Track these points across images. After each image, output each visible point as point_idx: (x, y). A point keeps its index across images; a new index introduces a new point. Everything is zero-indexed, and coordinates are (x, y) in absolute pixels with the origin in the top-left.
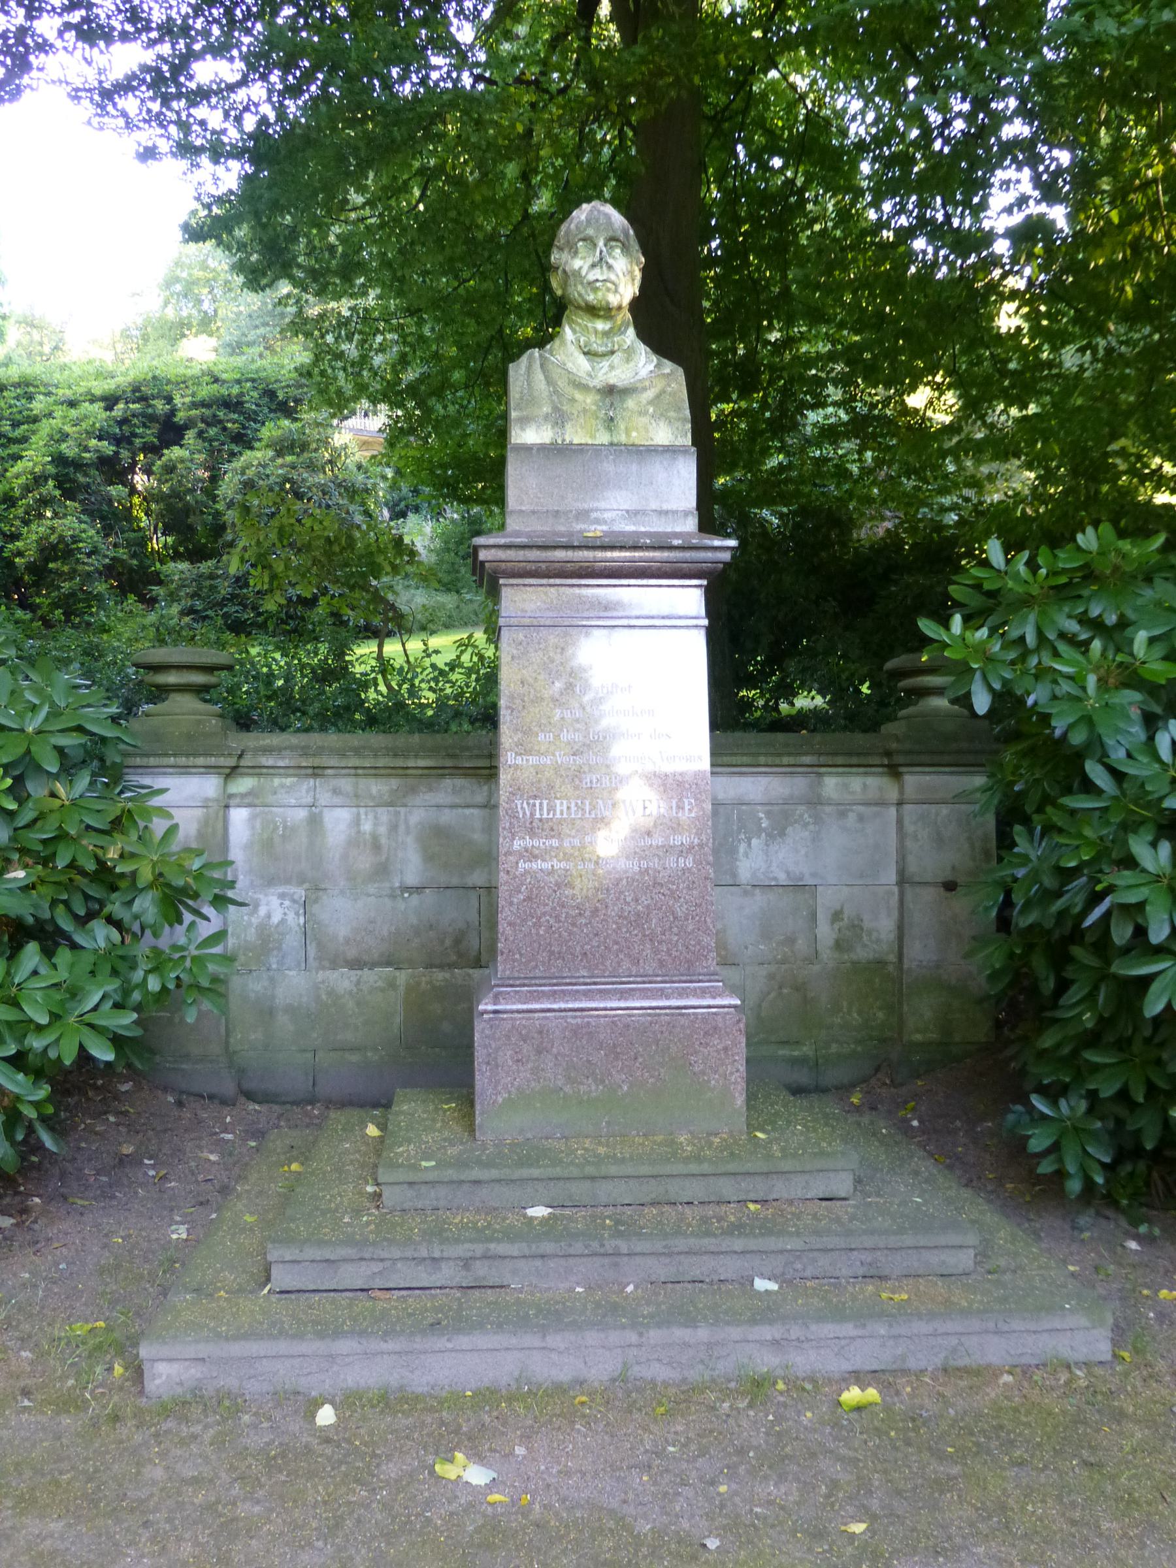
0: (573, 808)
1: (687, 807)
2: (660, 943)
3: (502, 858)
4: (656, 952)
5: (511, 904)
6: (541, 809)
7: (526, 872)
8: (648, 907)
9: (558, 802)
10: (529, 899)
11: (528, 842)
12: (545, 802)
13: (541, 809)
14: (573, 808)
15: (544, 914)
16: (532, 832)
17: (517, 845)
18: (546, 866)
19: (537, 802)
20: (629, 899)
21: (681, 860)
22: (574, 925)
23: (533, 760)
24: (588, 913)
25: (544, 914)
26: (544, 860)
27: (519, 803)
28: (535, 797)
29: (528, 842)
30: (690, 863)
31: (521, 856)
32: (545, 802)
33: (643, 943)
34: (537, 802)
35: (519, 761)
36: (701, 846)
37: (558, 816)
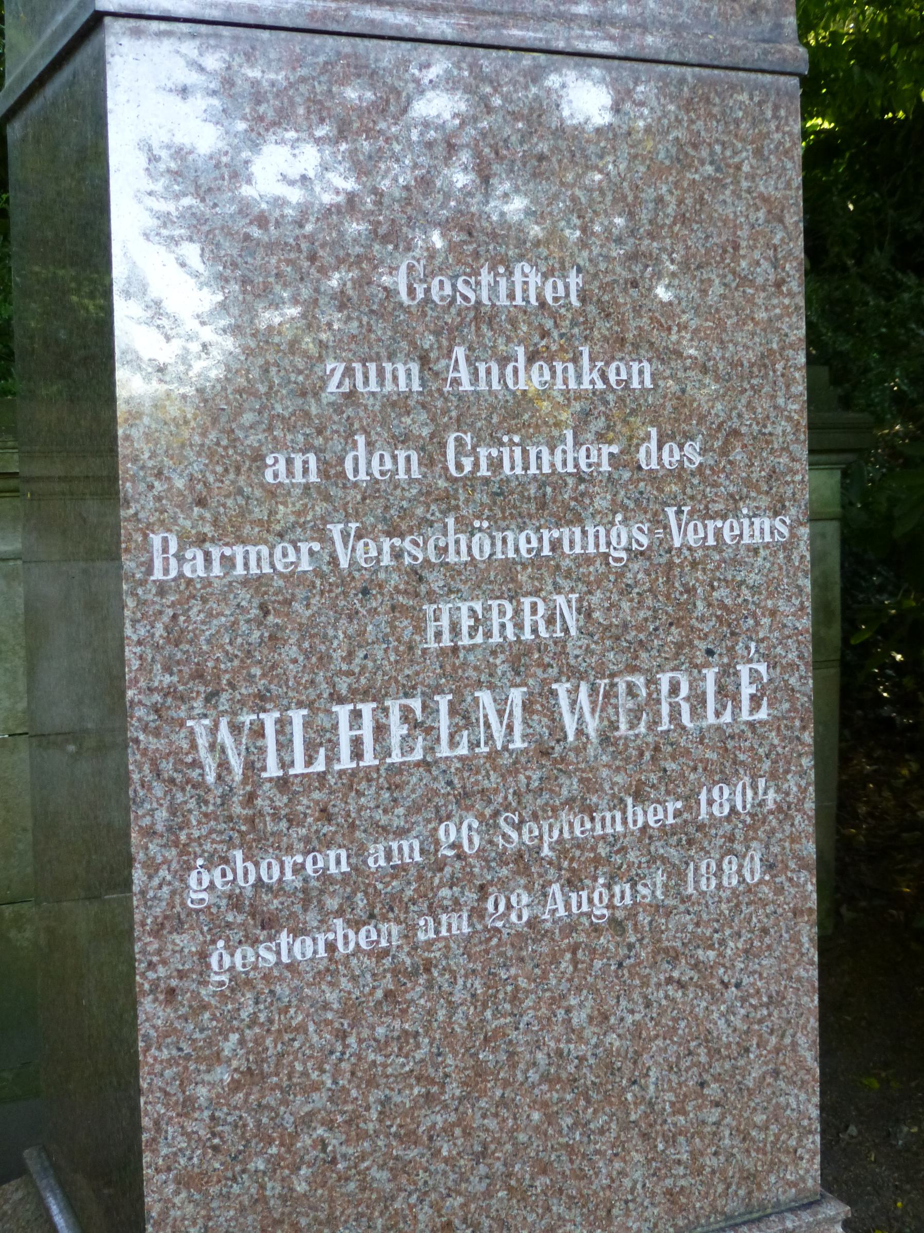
0: (397, 730)
1: (747, 690)
2: (670, 1140)
3: (145, 944)
4: (659, 1166)
5: (188, 1106)
6: (284, 745)
7: (240, 982)
8: (637, 1031)
9: (343, 712)
10: (251, 1077)
11: (243, 871)
12: (297, 716)
13: (284, 745)
14: (397, 730)
15: (307, 1121)
16: (256, 841)
17: (201, 886)
18: (304, 949)
19: (269, 720)
20: (579, 1018)
21: (730, 866)
22: (409, 1137)
23: (252, 558)
24: (454, 1089)
25: (307, 1121)
26: (298, 932)
27: (200, 727)
28: (261, 701)
29: (243, 871)
30: (754, 871)
31: (218, 928)
32: (297, 716)
33: (620, 1150)
34: (269, 720)
35: (195, 567)
36: (781, 809)
37: (346, 762)
